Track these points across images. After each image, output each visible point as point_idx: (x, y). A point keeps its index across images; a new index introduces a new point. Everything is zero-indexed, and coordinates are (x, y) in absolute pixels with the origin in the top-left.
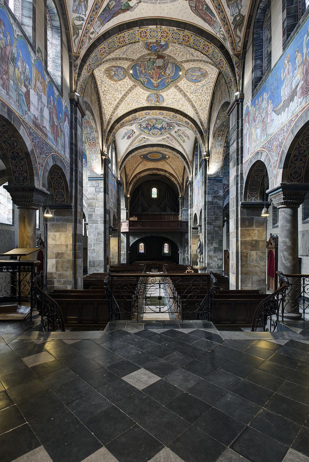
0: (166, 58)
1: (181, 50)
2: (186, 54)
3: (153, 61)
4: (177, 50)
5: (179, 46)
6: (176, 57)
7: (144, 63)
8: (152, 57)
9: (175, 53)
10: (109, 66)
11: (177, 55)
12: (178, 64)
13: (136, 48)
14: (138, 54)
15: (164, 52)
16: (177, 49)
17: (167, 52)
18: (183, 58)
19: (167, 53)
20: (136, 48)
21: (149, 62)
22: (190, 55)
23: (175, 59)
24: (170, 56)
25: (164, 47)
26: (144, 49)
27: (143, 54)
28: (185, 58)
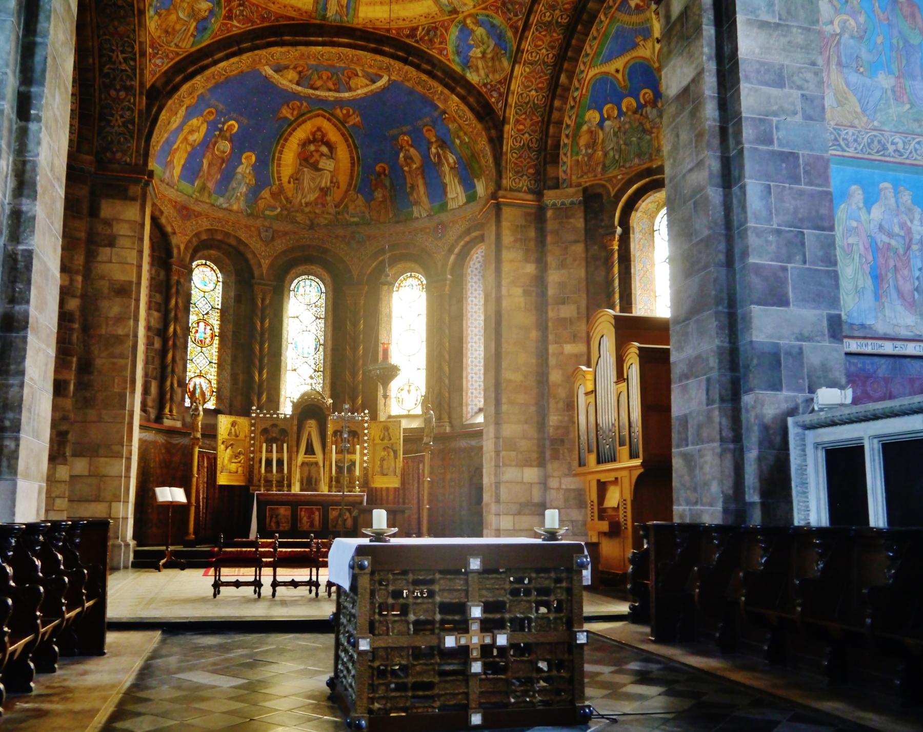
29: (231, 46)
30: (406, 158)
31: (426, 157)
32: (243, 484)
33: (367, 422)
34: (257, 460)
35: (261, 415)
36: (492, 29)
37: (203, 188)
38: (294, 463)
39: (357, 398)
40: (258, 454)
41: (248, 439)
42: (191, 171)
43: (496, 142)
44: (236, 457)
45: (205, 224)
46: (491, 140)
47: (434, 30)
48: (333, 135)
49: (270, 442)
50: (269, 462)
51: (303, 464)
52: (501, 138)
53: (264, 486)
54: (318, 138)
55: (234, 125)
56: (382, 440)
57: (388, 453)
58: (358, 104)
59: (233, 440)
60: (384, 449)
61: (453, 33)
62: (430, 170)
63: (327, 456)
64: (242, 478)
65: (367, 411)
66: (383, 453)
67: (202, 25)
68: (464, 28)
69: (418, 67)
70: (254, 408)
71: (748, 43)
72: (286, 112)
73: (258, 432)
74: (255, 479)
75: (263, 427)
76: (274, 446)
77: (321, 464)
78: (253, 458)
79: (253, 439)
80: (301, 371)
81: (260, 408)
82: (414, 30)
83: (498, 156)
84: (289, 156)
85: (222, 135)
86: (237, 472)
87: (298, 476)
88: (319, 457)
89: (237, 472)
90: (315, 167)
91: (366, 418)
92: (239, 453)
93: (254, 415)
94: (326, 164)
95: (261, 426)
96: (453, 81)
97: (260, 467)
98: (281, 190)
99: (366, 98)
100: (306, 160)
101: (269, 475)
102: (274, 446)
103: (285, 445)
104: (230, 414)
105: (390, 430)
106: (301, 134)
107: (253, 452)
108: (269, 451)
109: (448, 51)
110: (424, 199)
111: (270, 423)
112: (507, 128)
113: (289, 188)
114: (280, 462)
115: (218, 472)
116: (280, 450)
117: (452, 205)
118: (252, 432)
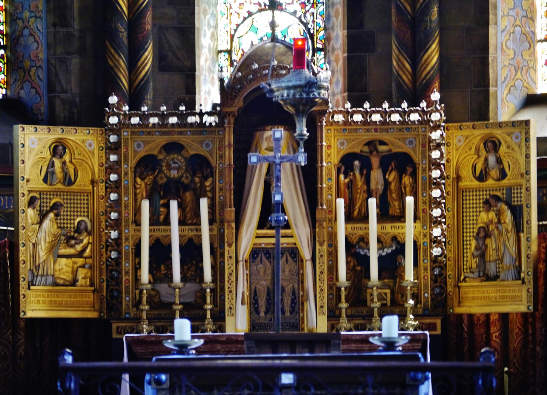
32: (93, 315)
33: (437, 127)
34: (127, 246)
35: (135, 120)
38: (229, 251)
39: (424, 47)
40: (130, 231)
41: (101, 189)
44: (69, 240)
49: (160, 194)
50: (160, 250)
51: (255, 253)
53: (150, 320)
56: (482, 178)
57: (499, 214)
59: (57, 193)
60: (488, 205)
63: (323, 232)
64: (90, 298)
65: (435, 96)
66: (485, 217)
70: (113, 99)
73: (128, 167)
74: (126, 300)
75: (143, 152)
76: (174, 205)
77: (306, 254)
78: (118, 241)
79: (116, 186)
81: (135, 100)
86: (74, 282)
87: (243, 288)
88: (301, 233)
89: (74, 282)
91: (435, 117)
92: (78, 230)
93: (114, 120)
95: (136, 150)
97: (137, 267)
101: (163, 288)
102: (174, 205)
103: (204, 203)
104: (51, 120)
105: (503, 149)
107: (116, 225)
108: (160, 220)
111: (163, 140)
114: (192, 250)
115: (23, 284)
116: (190, 218)
118: (111, 168)
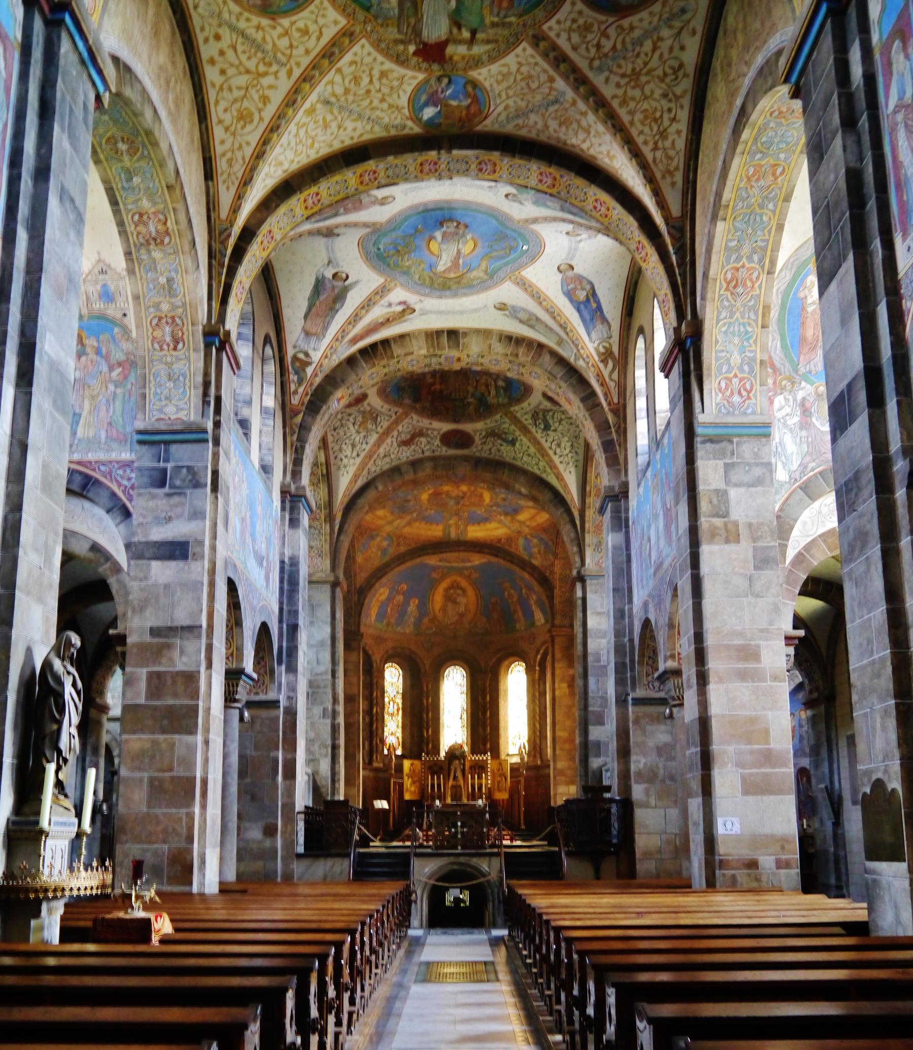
0: (412, 48)
1: (368, 101)
2: (347, 91)
3: (459, 27)
4: (380, 95)
5: (378, 113)
6: (375, 59)
7: (496, 11)
8: (462, 50)
9: (384, 81)
10: (634, 19)
11: (376, 73)
12: (361, 15)
13: (515, 95)
14: (514, 69)
15: (421, 76)
16: (383, 100)
17: (414, 78)
18: (352, 63)
19: (410, 73)
20: (515, 95)
21: (474, 21)
22: (336, 96)
23: (376, 45)
24: (400, 60)
25: (424, 98)
26: (489, 88)
27: (495, 68)
28: (347, 70)
29: (400, 559)
30: (509, 594)
31: (520, 595)
36: (541, 540)
37: (388, 624)
42: (381, 615)
43: (551, 597)
45: (390, 644)
46: (548, 597)
47: (510, 540)
48: (464, 583)
52: (553, 596)
54: (455, 586)
55: (405, 587)
58: (477, 568)
61: (521, 542)
62: (523, 602)
67: (384, 551)
68: (526, 539)
69: (504, 559)
71: (592, 622)
72: (434, 575)
80: (453, 730)
82: (499, 540)
83: (552, 606)
84: (438, 599)
85: (398, 593)
90: (455, 602)
94: (462, 600)
96: (524, 565)
98: (435, 617)
99: (481, 565)
100: (449, 598)
106: (444, 585)
109: (520, 547)
110: (522, 619)
112: (556, 591)
113: (440, 615)
117: (538, 623)
